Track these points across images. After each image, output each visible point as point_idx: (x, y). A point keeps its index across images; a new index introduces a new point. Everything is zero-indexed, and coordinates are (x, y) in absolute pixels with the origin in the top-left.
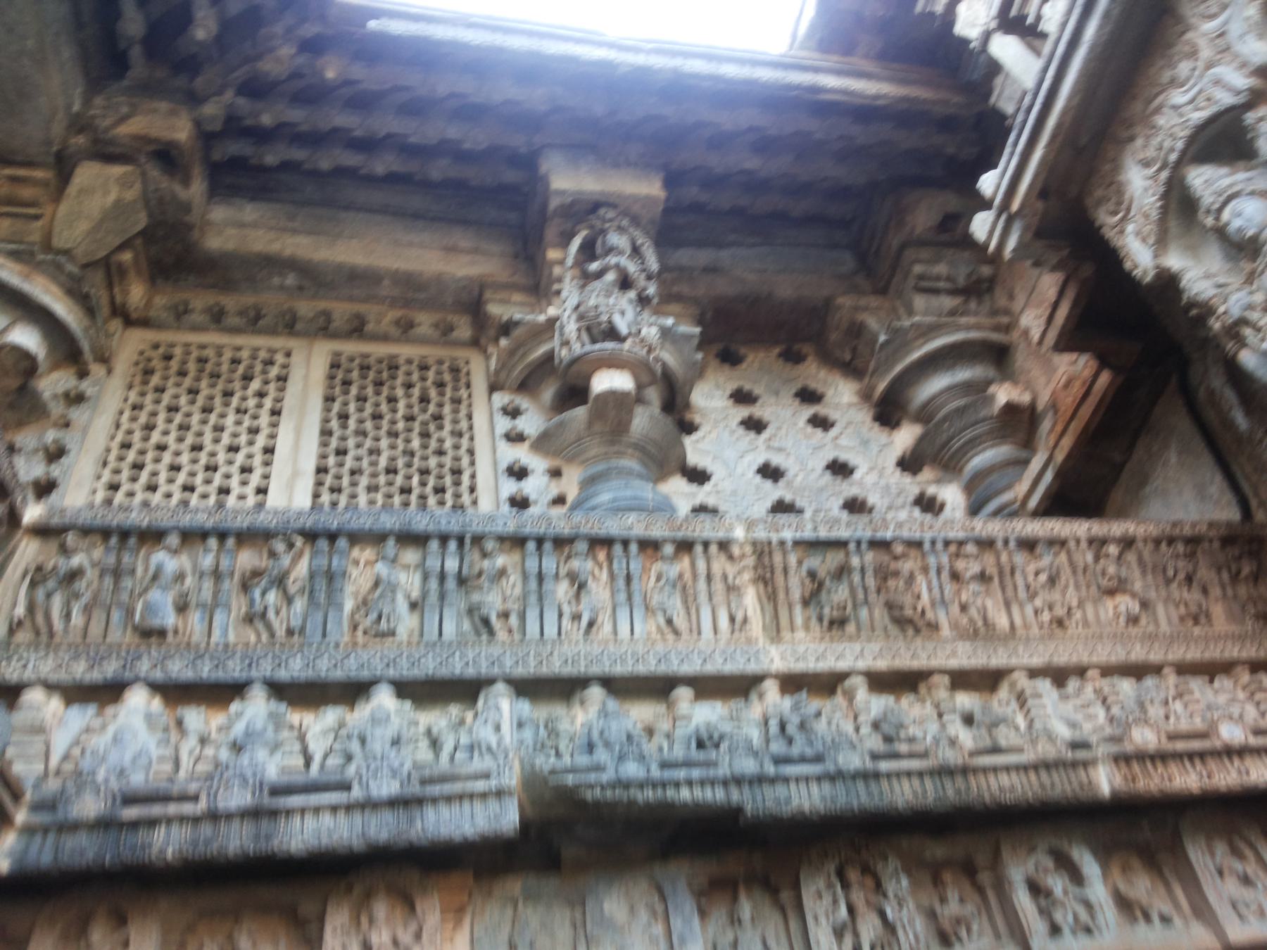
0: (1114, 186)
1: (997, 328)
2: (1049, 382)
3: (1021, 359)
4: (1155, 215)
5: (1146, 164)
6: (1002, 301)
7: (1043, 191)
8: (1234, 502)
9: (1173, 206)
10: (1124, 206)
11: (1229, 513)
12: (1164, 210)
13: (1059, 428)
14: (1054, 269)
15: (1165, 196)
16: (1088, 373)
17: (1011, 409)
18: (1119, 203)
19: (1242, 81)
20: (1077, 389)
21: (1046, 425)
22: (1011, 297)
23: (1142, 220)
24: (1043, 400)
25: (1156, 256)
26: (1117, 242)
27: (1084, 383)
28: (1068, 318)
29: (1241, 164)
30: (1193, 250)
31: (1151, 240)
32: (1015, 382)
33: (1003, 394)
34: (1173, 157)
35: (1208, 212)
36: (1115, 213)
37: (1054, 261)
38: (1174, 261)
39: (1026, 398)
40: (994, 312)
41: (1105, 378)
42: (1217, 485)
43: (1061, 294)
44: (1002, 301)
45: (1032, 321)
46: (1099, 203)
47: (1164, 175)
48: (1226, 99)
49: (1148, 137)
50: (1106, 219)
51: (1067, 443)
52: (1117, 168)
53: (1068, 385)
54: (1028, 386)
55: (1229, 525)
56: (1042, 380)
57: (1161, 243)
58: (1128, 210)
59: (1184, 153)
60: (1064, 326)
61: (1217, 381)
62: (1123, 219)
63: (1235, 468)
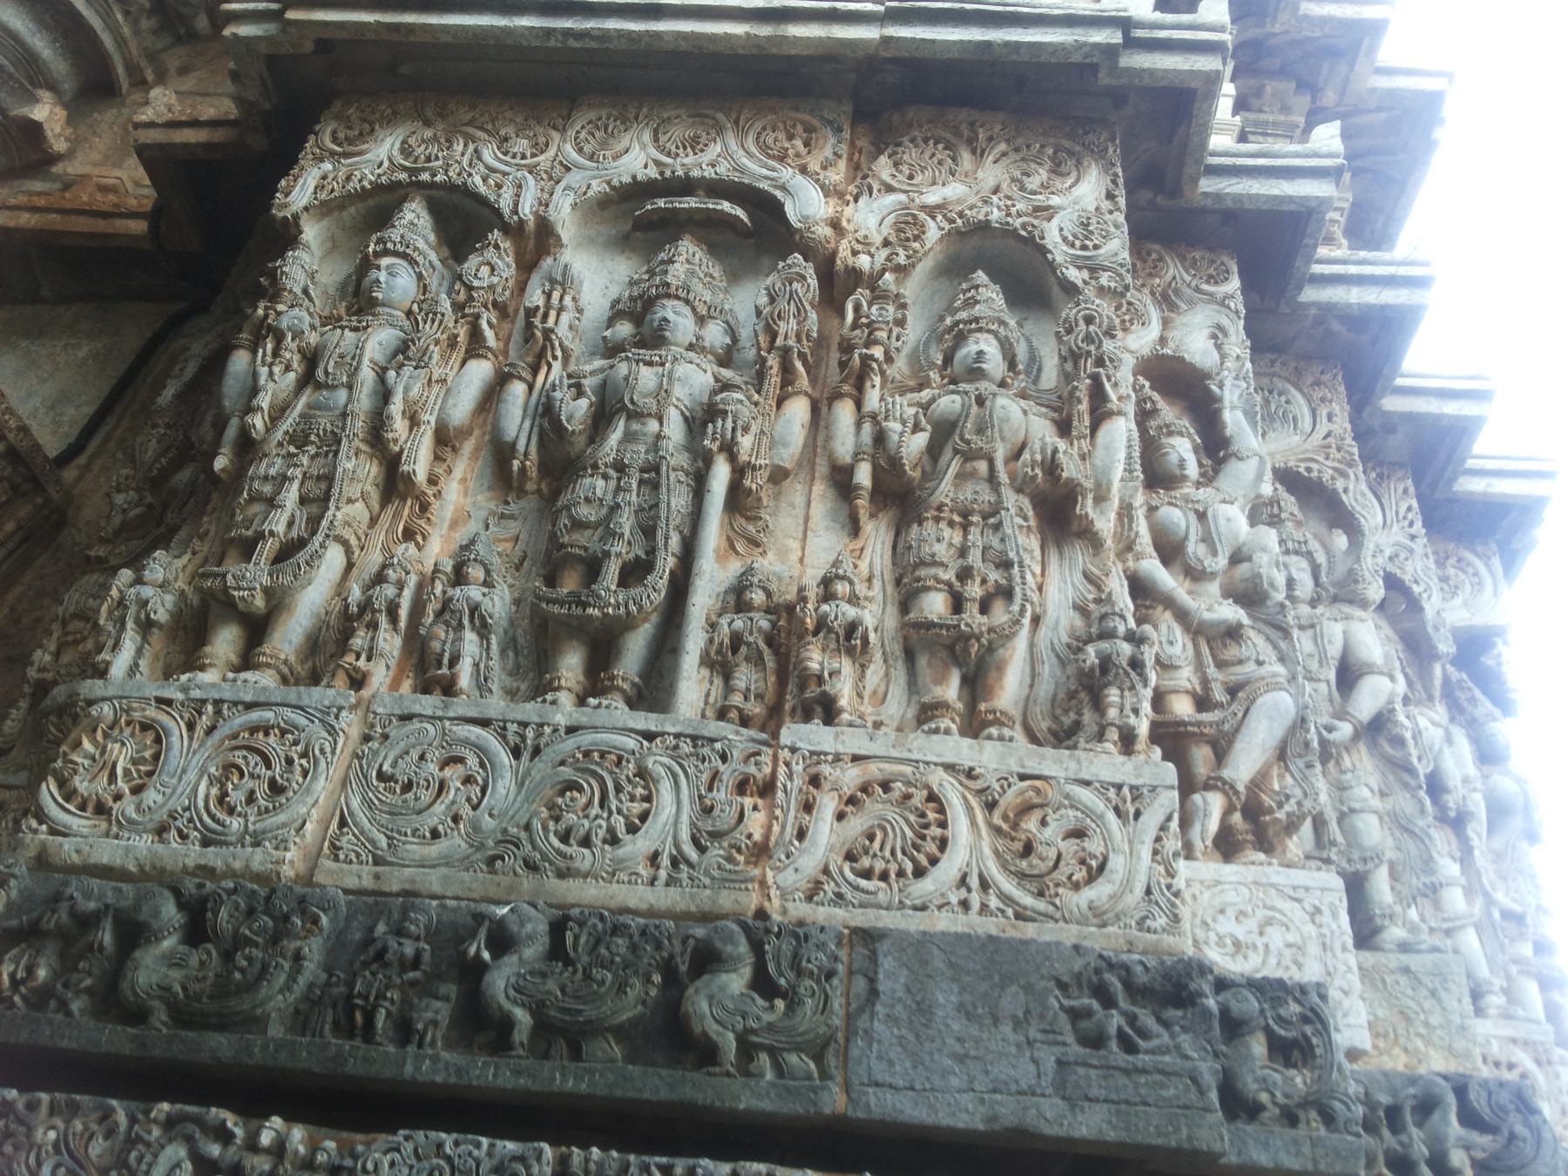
0: (367, 127)
1: (132, 69)
2: (94, 164)
3: (108, 119)
4: (353, 185)
5: (406, 151)
6: (172, 62)
7: (328, 42)
8: (72, 439)
9: (370, 202)
10: (352, 149)
11: (52, 446)
12: (363, 195)
13: (41, 202)
14: (239, 100)
15: (378, 188)
16: (132, 203)
17: (34, 130)
18: (350, 141)
19: (527, 209)
20: (106, 202)
21: (37, 186)
22: (183, 71)
23: (341, 175)
24: (73, 168)
25: (306, 209)
26: (305, 158)
27: (116, 206)
28: (185, 145)
29: (446, 252)
30: (333, 247)
31: (323, 196)
32: (70, 121)
33: (45, 111)
34: (425, 177)
35: (380, 241)
36: (335, 140)
37: (252, 94)
38: (311, 232)
39: (60, 146)
40: (152, 57)
41: (138, 227)
42: (77, 414)
43: (213, 124)
44: (172, 62)
45: (161, 103)
46: (337, 117)
47: (403, 176)
48: (505, 204)
49: (435, 139)
50: (326, 135)
51: (26, 220)
52: (390, 121)
53: (104, 189)
54: (76, 143)
55: (37, 447)
56: (96, 156)
57: (323, 209)
58: (347, 155)
59: (433, 185)
60: (172, 145)
61: (199, 349)
62: (333, 154)
63: (111, 421)
